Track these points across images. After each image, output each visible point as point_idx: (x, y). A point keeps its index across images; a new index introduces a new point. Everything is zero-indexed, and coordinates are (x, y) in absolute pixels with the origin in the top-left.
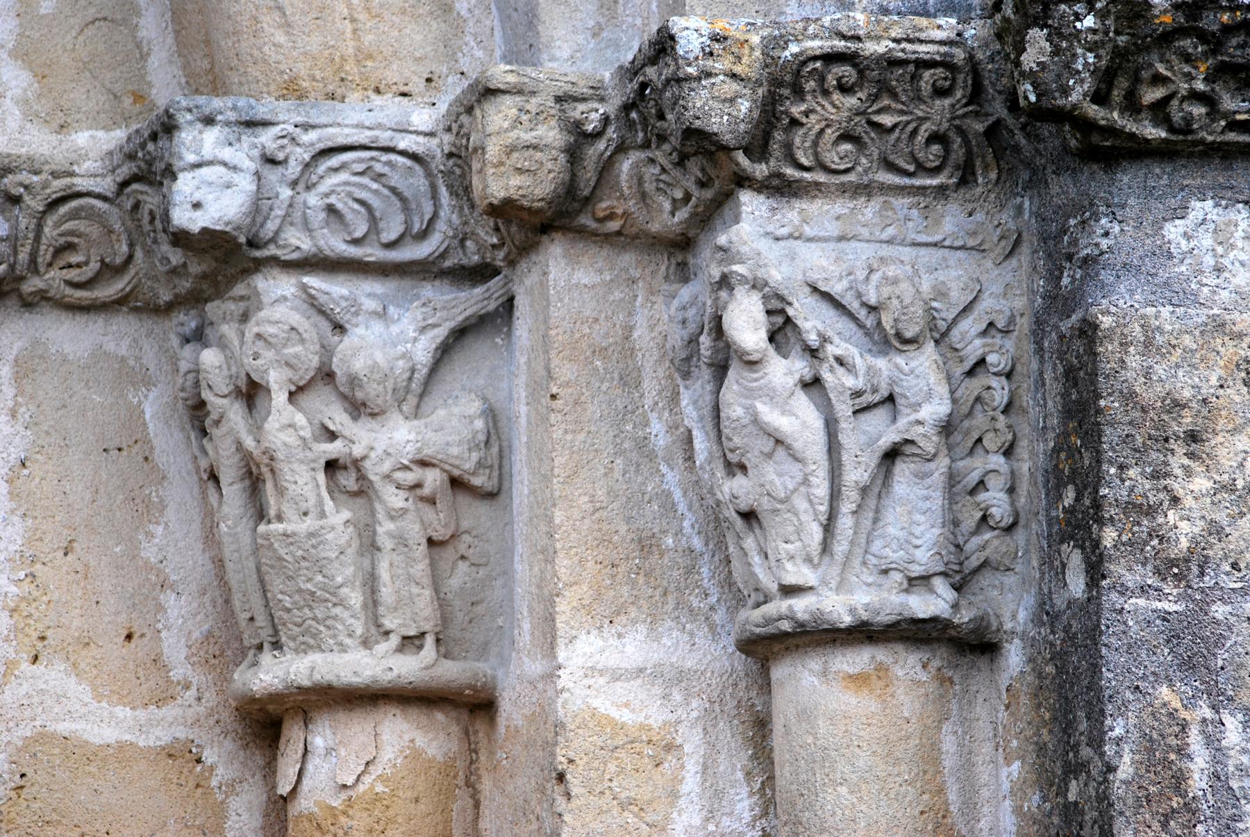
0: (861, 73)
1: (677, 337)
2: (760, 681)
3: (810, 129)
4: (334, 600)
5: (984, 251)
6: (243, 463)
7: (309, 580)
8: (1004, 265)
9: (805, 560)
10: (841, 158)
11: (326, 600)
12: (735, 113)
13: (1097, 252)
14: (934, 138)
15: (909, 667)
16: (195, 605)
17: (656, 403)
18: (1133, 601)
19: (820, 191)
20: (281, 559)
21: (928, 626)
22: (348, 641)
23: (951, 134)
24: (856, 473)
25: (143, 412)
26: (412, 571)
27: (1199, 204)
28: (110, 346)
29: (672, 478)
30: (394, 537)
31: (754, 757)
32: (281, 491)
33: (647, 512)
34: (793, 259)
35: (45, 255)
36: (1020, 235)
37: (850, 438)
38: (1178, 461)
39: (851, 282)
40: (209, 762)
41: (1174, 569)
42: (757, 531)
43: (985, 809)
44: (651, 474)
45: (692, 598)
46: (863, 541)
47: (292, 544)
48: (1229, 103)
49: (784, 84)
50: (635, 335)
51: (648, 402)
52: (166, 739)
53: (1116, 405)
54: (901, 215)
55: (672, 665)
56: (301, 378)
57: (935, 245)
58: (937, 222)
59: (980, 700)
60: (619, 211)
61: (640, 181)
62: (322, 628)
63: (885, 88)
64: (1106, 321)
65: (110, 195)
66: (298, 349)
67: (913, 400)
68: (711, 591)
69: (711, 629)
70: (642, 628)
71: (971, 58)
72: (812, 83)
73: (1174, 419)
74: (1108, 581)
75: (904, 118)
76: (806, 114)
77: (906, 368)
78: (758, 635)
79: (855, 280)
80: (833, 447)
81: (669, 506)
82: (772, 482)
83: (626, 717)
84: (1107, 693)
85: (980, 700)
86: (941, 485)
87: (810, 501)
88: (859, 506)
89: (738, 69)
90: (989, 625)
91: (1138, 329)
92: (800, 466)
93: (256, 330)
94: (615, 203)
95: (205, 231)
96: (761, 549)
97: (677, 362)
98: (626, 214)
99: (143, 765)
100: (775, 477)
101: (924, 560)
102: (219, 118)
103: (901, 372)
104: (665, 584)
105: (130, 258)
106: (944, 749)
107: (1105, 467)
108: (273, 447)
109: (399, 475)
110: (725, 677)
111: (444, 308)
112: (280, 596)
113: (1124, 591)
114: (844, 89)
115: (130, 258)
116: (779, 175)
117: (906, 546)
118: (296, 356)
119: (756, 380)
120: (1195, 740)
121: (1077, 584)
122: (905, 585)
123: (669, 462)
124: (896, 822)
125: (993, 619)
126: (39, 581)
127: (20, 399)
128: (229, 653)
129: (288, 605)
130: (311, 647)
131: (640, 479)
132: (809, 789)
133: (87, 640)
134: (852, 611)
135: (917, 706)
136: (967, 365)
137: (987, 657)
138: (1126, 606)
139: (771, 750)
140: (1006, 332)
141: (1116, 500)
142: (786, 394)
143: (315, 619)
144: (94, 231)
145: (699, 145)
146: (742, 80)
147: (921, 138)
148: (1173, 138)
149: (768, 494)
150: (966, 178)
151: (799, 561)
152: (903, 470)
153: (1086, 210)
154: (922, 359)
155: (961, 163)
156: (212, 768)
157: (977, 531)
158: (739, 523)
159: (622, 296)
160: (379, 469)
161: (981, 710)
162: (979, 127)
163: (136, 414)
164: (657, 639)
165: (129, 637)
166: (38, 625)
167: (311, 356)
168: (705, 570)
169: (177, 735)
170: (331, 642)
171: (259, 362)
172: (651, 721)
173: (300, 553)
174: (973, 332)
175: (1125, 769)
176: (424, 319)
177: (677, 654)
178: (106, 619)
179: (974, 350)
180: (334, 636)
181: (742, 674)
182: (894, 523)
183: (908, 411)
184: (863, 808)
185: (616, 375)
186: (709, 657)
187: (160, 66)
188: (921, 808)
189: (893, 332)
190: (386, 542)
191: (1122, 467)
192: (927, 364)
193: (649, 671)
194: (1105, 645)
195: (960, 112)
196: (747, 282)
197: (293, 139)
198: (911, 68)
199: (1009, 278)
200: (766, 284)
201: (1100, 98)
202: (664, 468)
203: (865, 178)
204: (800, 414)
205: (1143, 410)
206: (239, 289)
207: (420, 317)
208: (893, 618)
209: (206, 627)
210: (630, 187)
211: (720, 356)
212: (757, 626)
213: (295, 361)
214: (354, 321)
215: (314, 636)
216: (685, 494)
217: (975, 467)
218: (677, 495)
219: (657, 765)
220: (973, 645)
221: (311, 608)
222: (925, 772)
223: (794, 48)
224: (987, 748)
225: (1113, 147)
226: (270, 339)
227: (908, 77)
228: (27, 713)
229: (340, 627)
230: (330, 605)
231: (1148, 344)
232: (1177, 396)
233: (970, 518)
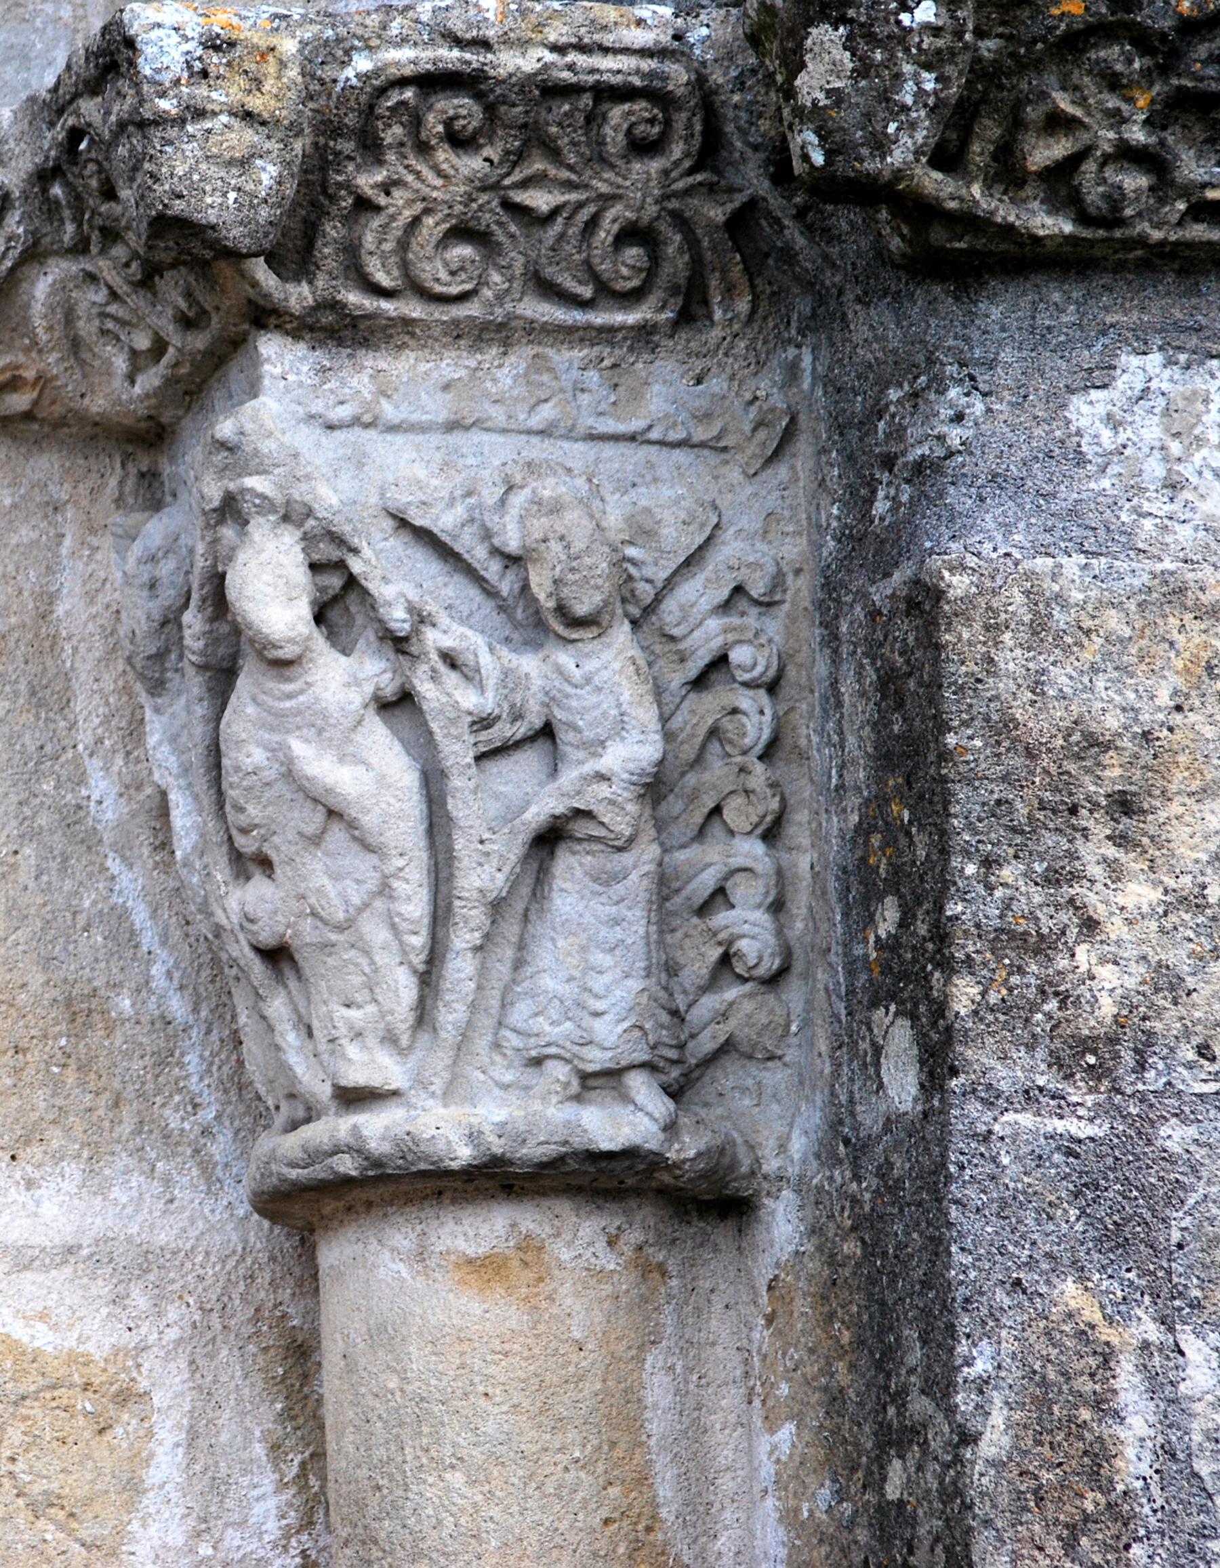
0: (490, 110)
1: (140, 614)
2: (297, 1271)
3: (393, 218)
5: (725, 449)
8: (764, 476)
9: (383, 1040)
10: (453, 273)
12: (250, 187)
13: (940, 452)
14: (629, 234)
15: (580, 1242)
17: (100, 741)
18: (1009, 1117)
19: (412, 335)
21: (619, 1166)
23: (663, 227)
24: (482, 873)
27: (1135, 361)
29: (130, 883)
31: (287, 1415)
33: (83, 948)
34: (360, 465)
36: (793, 420)
37: (469, 807)
38: (1095, 851)
39: (471, 509)
41: (1088, 1056)
42: (293, 984)
43: (727, 1514)
44: (90, 876)
45: (167, 1112)
46: (495, 1003)
48: (1192, 167)
49: (344, 131)
50: (60, 610)
51: (84, 738)
53: (978, 743)
54: (566, 381)
55: (129, 1239)
57: (632, 438)
58: (636, 395)
59: (718, 1307)
60: (30, 374)
61: (69, 317)
63: (534, 139)
64: (958, 585)
67: (589, 734)
68: (204, 1099)
69: (204, 1171)
70: (73, 1169)
71: (700, 81)
72: (398, 130)
73: (1088, 771)
74: (962, 1079)
75: (574, 196)
76: (386, 188)
77: (577, 674)
79: (480, 506)
80: (437, 824)
81: (123, 937)
82: (320, 891)
83: (42, 1338)
84: (961, 1293)
85: (718, 1307)
86: (643, 896)
87: (393, 926)
88: (487, 937)
89: (256, 103)
90: (734, 1164)
91: (1019, 598)
92: (373, 859)
94: (22, 358)
96: (300, 1018)
97: (139, 662)
98: (42, 380)
100: (326, 881)
101: (611, 1040)
103: (568, 680)
104: (116, 1084)
106: (649, 1401)
107: (956, 862)
110: (231, 1263)
113: (992, 1099)
114: (459, 141)
116: (334, 305)
117: (579, 1013)
119: (290, 696)
120: (1128, 1382)
121: (902, 1086)
122: (575, 1087)
123: (123, 851)
124: (558, 1540)
125: (742, 1152)
131: (68, 885)
132: (391, 1478)
134: (473, 1136)
135: (598, 1317)
136: (694, 668)
137: (731, 1223)
138: (997, 1128)
139: (320, 1402)
140: (767, 605)
141: (978, 926)
142: (347, 723)
145: (182, 247)
146: (263, 123)
147: (604, 235)
148: (1087, 233)
149: (314, 914)
150: (691, 310)
151: (371, 1040)
152: (570, 867)
153: (921, 373)
154: (607, 656)
155: (682, 282)
157: (712, 984)
158: (257, 968)
159: (34, 535)
161: (719, 1326)
162: (717, 213)
164: (102, 1191)
168: (192, 1060)
172: (90, 1347)
174: (705, 604)
175: (995, 1439)
177: (140, 1218)
179: (708, 636)
181: (263, 1257)
182: (553, 969)
183: (581, 755)
184: (495, 1512)
185: (23, 687)
186: (200, 1224)
188: (604, 1513)
189: (551, 604)
191: (988, 863)
192: (617, 665)
193: (85, 1252)
194: (957, 1202)
195: (680, 185)
196: (273, 509)
198: (586, 100)
199: (772, 501)
200: (310, 513)
201: (946, 157)
202: (114, 865)
203: (498, 311)
204: (374, 761)
205: (1030, 754)
208: (552, 1150)
210: (50, 329)
211: (222, 651)
212: (293, 1165)
216: (154, 914)
217: (707, 863)
218: (140, 915)
219: (101, 1431)
220: (704, 1202)
222: (613, 1444)
223: (362, 63)
224: (731, 1398)
225: (971, 252)
227: (580, 119)
231: (1038, 627)
232: (1094, 727)
233: (699, 960)
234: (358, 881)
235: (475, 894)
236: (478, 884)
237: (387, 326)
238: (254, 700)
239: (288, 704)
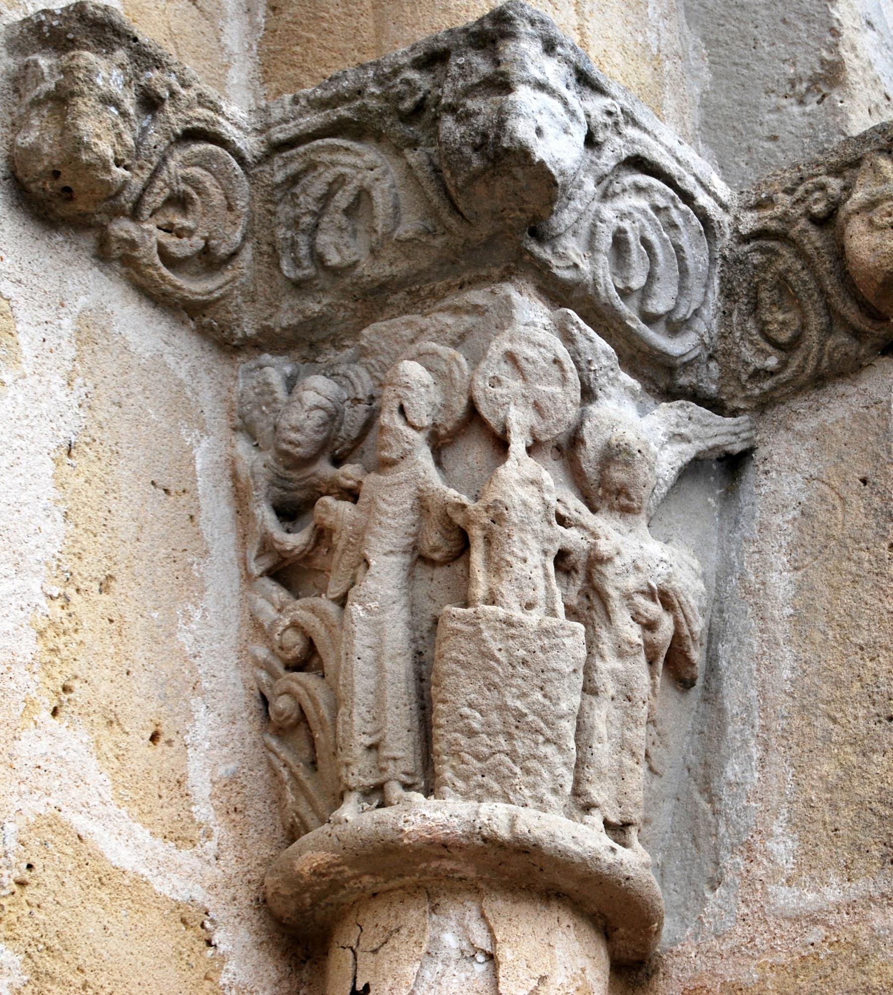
4: (548, 733)
6: (413, 530)
7: (523, 695)
11: (538, 731)
16: (223, 731)
20: (488, 655)
22: (550, 797)
25: (194, 458)
26: (628, 734)
28: (170, 360)
30: (619, 681)
32: (496, 568)
35: (156, 199)
40: (222, 948)
47: (513, 637)
52: (181, 896)
56: (547, 430)
62: (517, 770)
65: (249, 158)
66: (557, 389)
93: (507, 346)
95: (542, 163)
99: (154, 917)
102: (559, 49)
105: (234, 255)
108: (507, 501)
109: (640, 600)
111: (699, 421)
112: (466, 710)
115: (234, 255)
118: (552, 398)
126: (72, 609)
127: (78, 367)
128: (251, 813)
129: (475, 725)
130: (491, 794)
133: (112, 717)
143: (512, 755)
144: (217, 197)
156: (223, 959)
160: (621, 583)
163: (186, 458)
165: (154, 738)
166: (65, 669)
167: (570, 405)
169: (194, 894)
170: (527, 792)
171: (498, 390)
173: (522, 653)
176: (678, 425)
178: (137, 700)
180: (534, 786)
187: (237, 84)
190: (610, 687)
197: (616, 124)
206: (477, 296)
207: (673, 420)
209: (232, 766)
213: (549, 404)
214: (610, 389)
215: (501, 779)
221: (510, 737)
226: (523, 363)
228: (43, 782)
229: (546, 775)
230: (541, 739)
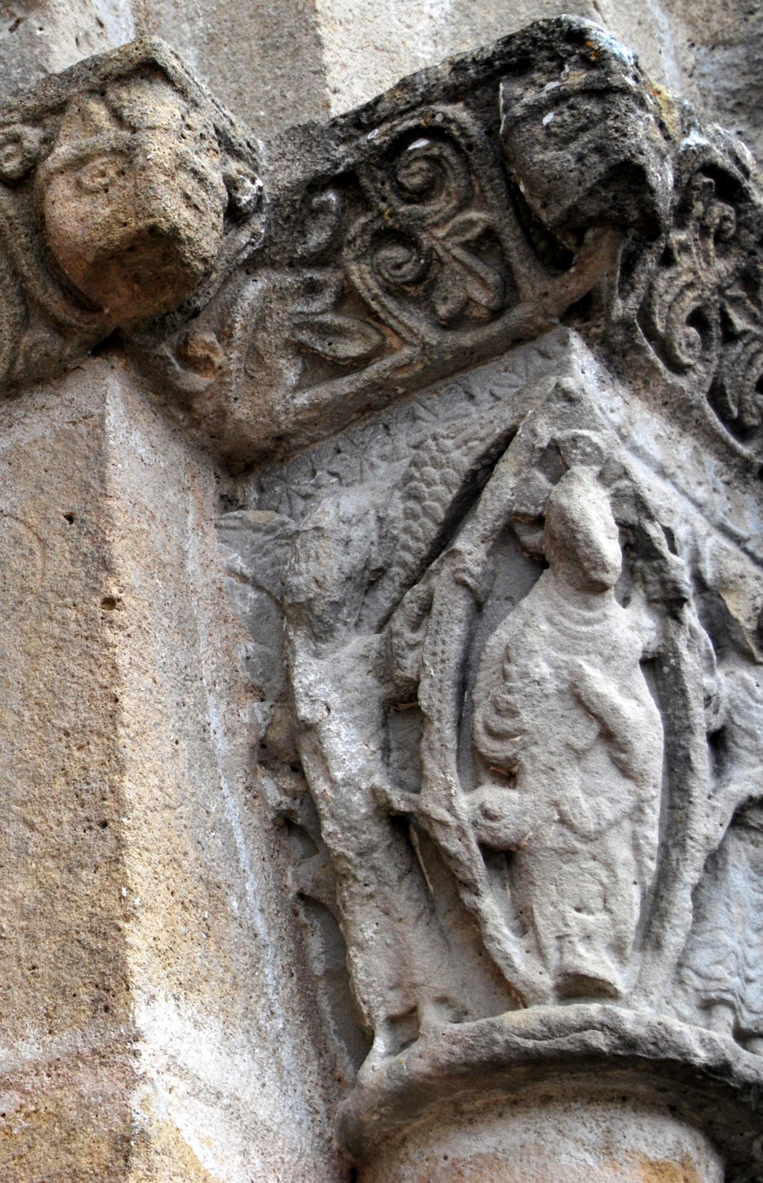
78: (527, 1052)
82: (575, 801)
92: (630, 785)
100: (578, 793)
119: (588, 622)
149: (563, 821)
212: (527, 1036)
234: (612, 800)
235: (701, 839)
236: (704, 831)
237: (641, 368)
238: (550, 620)
239: (584, 629)
